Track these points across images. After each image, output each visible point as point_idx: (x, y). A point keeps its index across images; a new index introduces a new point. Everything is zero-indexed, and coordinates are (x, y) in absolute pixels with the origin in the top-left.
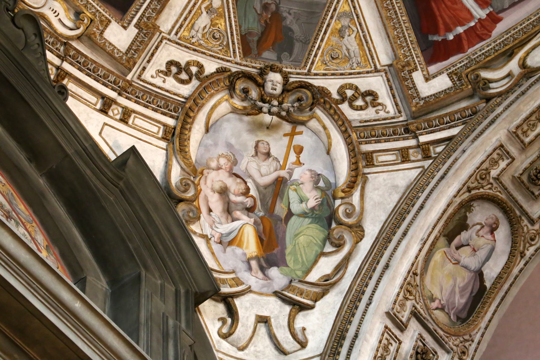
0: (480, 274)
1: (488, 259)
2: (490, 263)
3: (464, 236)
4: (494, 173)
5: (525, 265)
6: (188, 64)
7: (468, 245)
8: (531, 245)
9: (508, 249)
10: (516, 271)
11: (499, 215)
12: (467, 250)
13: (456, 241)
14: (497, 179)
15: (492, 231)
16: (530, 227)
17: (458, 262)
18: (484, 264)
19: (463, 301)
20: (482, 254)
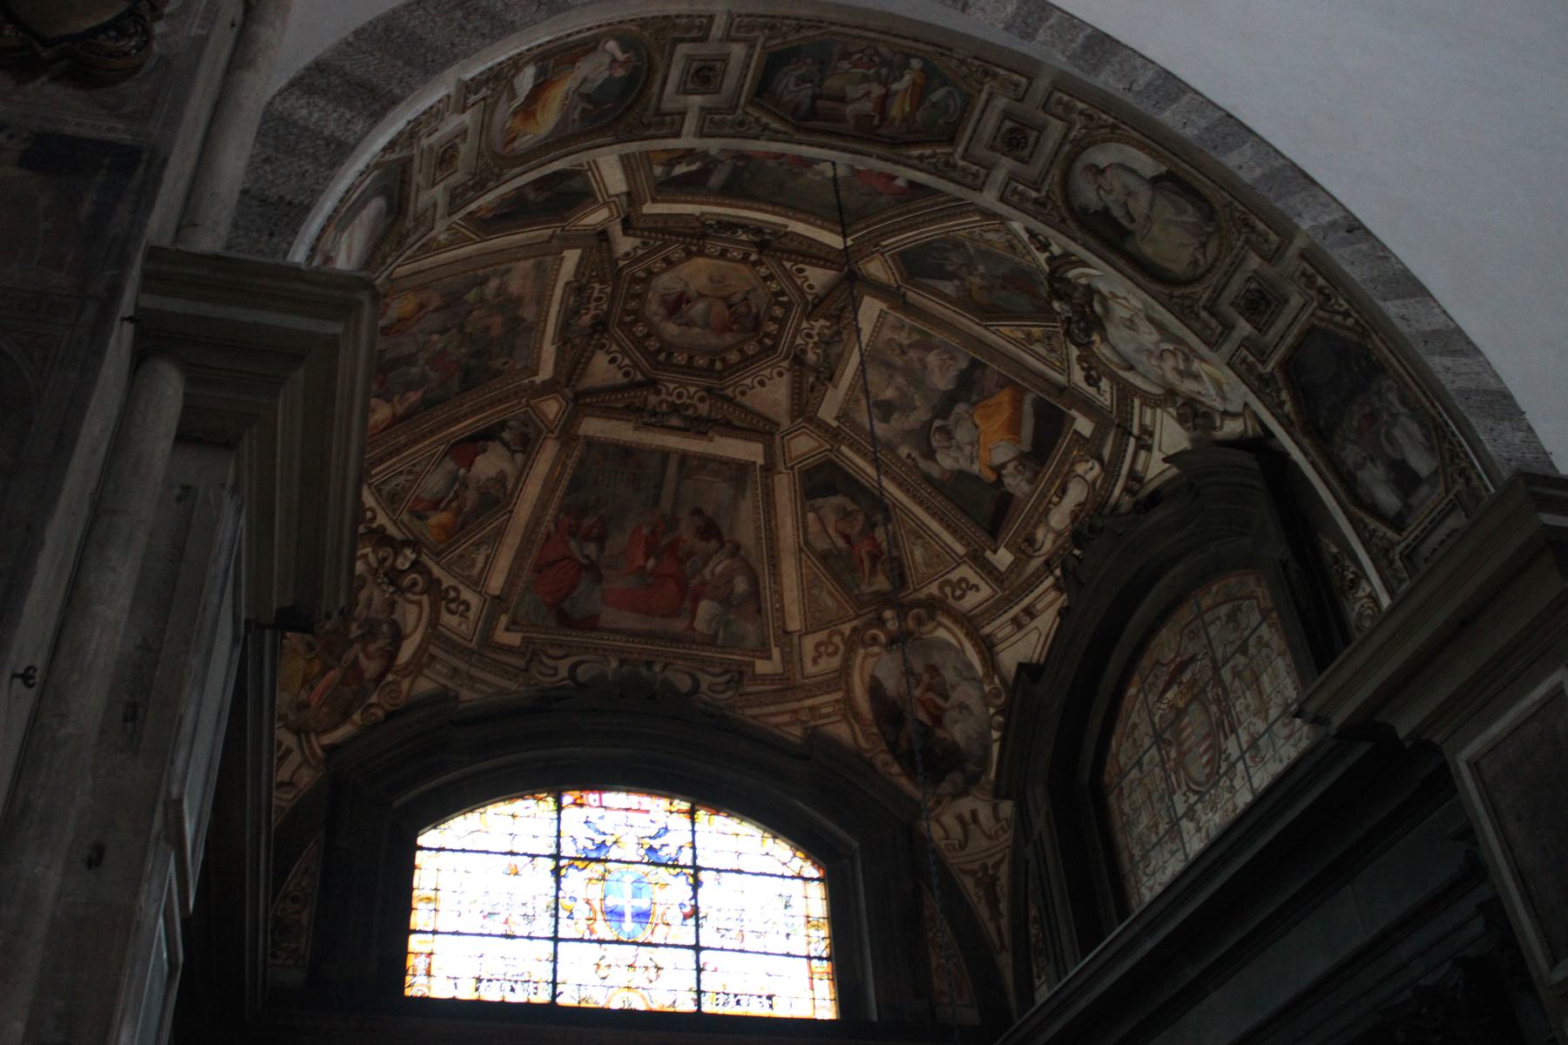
0: (1155, 181)
1: (1133, 172)
2: (1137, 166)
3: (1117, 212)
4: (1034, 194)
5: (1125, 124)
6: (1083, 369)
7: (1125, 204)
8: (1100, 118)
9: (1113, 145)
10: (1136, 134)
11: (1079, 165)
12: (1131, 203)
13: (1125, 222)
14: (1038, 190)
15: (1102, 171)
16: (1078, 126)
17: (1148, 218)
18: (1141, 177)
19: (1191, 209)
20: (1131, 181)
